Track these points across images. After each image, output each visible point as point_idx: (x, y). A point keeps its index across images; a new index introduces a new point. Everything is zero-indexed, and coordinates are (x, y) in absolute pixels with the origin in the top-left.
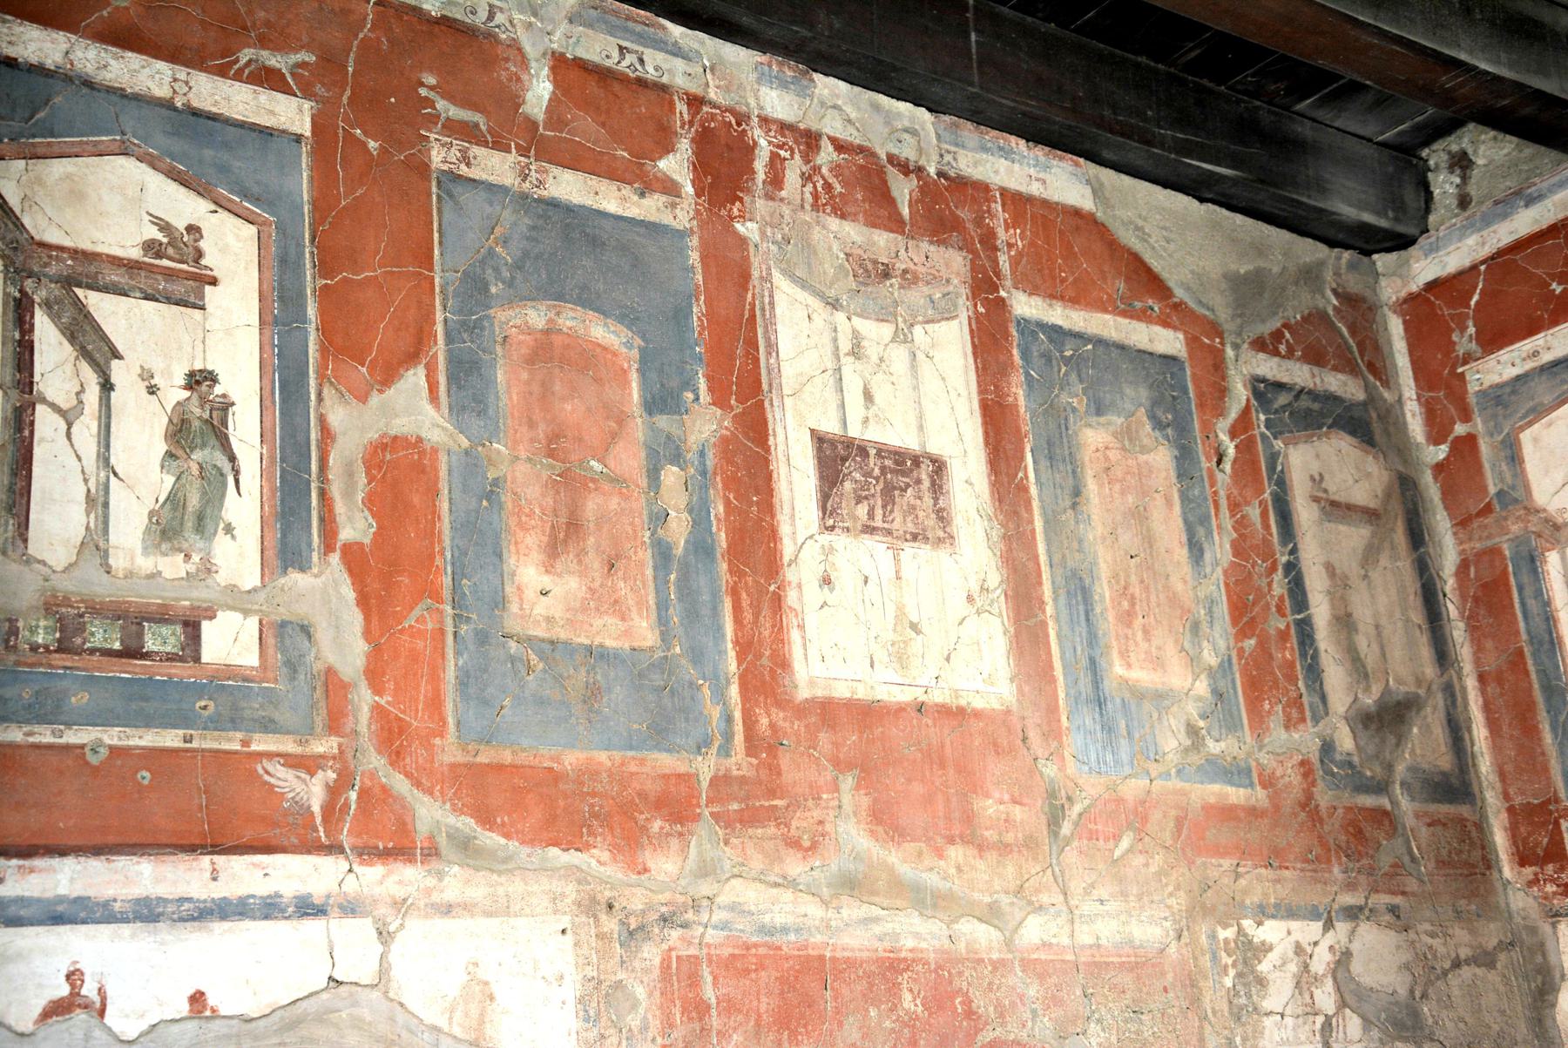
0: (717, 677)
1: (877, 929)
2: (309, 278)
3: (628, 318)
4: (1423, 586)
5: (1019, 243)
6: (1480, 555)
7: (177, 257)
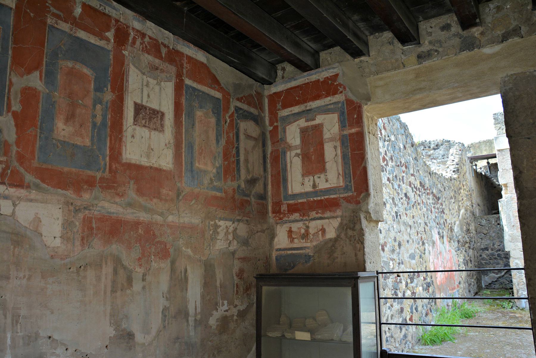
1: (135, 215)
4: (264, 155)
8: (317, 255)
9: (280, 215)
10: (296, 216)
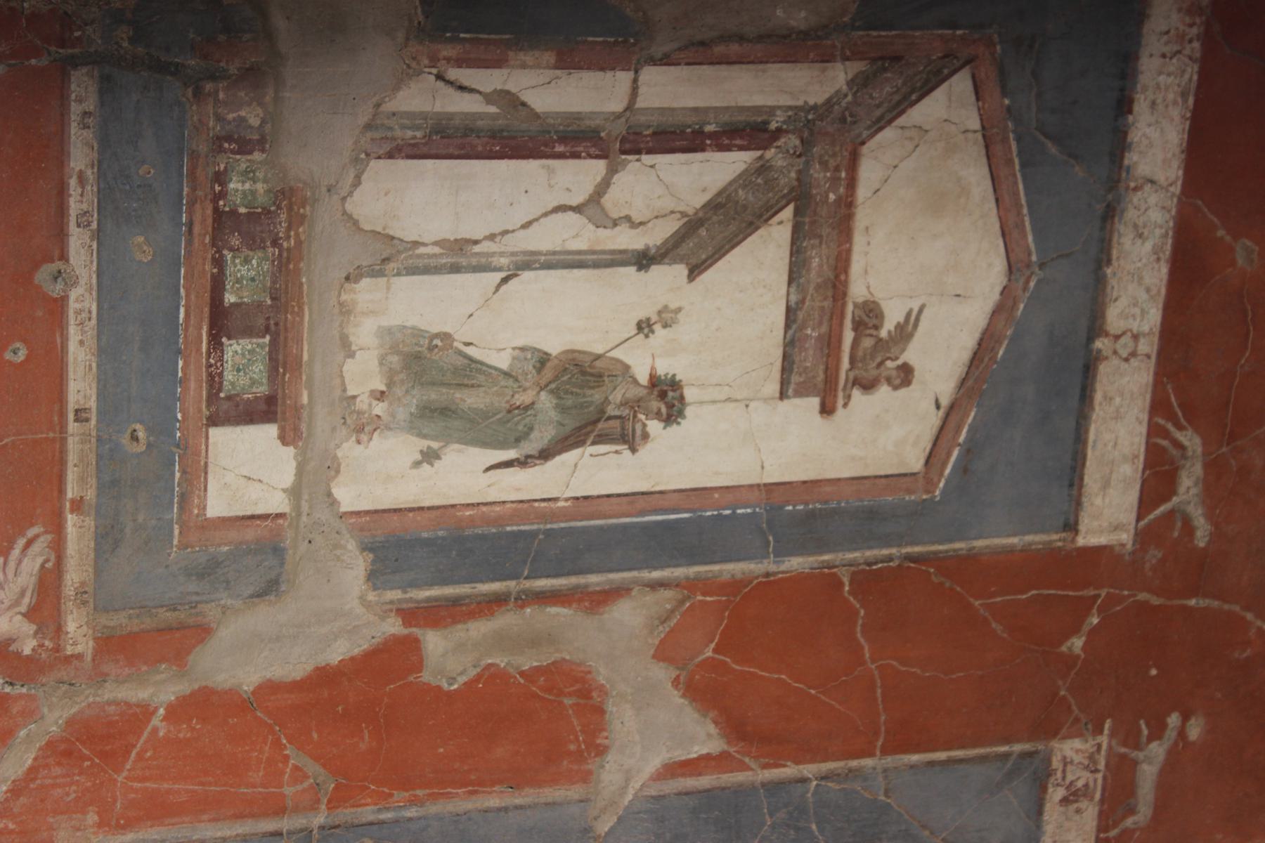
7: (860, 353)
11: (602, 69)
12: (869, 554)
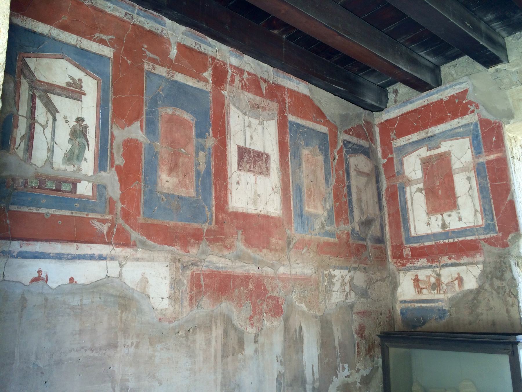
0: (209, 205)
1: (244, 269)
2: (110, 95)
3: (193, 113)
4: (378, 192)
5: (291, 102)
6: (392, 186)
7: (75, 87)
8: (454, 309)
9: (402, 260)
10: (423, 261)
11: (18, 121)
12: (110, 92)
